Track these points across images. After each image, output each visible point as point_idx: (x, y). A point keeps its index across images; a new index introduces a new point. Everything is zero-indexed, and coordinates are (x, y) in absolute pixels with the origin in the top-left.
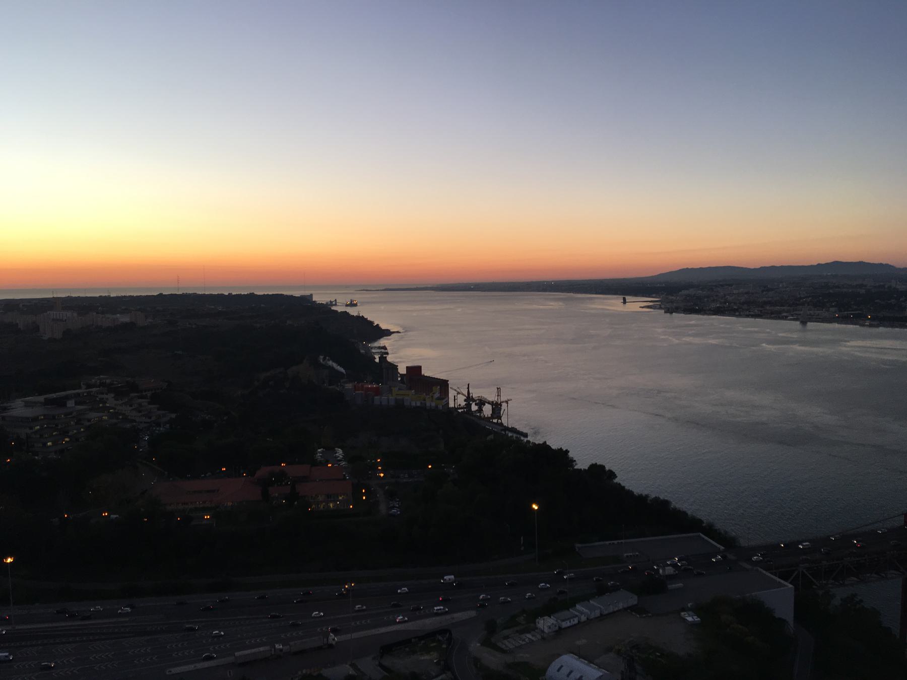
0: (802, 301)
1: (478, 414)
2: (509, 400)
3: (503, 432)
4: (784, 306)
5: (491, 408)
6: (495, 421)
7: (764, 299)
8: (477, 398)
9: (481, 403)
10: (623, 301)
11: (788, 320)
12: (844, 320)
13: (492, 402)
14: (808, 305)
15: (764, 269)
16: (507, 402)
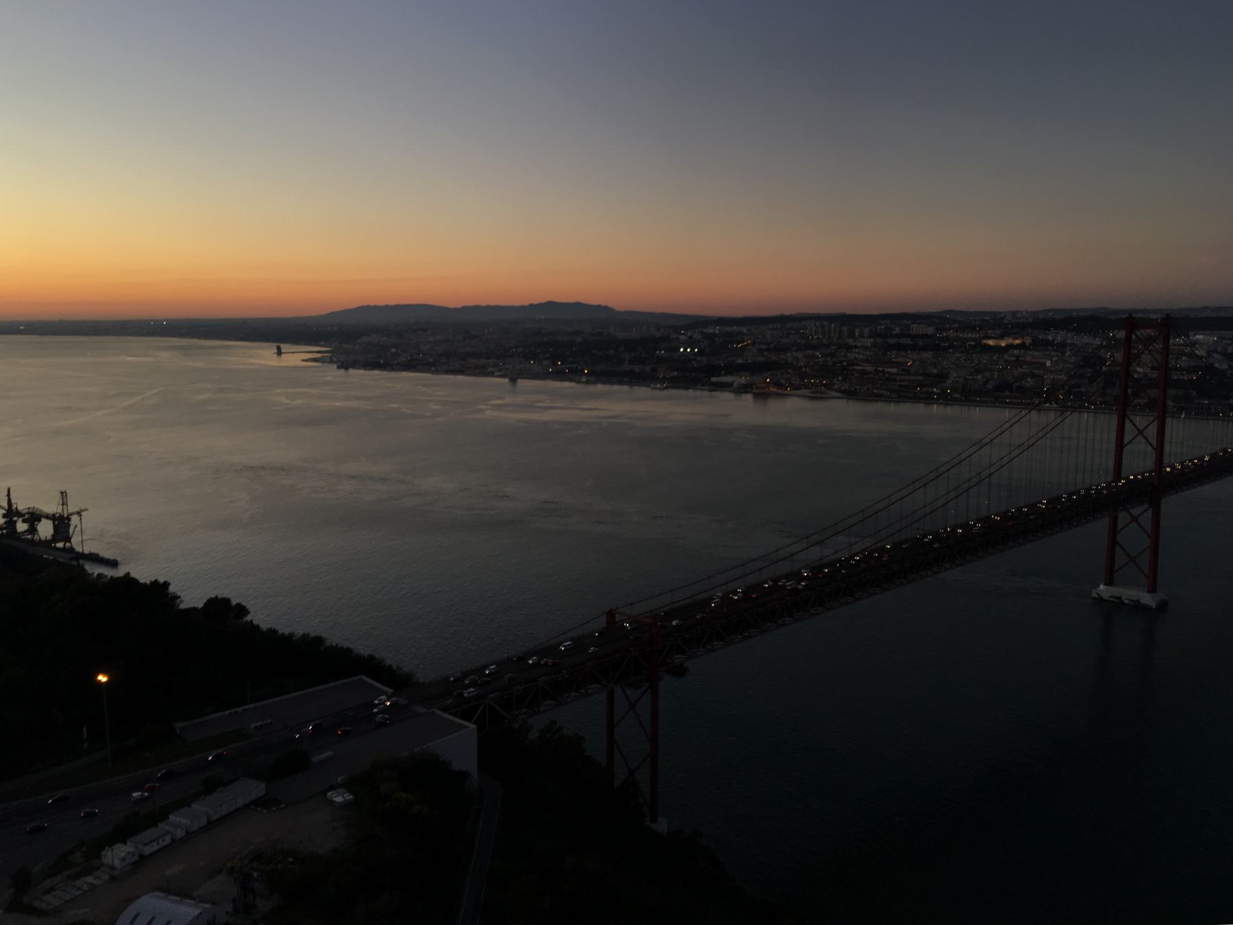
0: (511, 351)
1: (29, 537)
2: (82, 511)
3: (74, 563)
4: (490, 358)
5: (52, 525)
6: (60, 545)
7: (467, 349)
8: (25, 511)
9: (34, 518)
10: (276, 351)
11: (495, 377)
12: (559, 375)
13: (54, 515)
14: (519, 357)
15: (465, 309)
16: (79, 513)
